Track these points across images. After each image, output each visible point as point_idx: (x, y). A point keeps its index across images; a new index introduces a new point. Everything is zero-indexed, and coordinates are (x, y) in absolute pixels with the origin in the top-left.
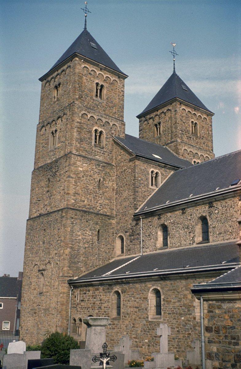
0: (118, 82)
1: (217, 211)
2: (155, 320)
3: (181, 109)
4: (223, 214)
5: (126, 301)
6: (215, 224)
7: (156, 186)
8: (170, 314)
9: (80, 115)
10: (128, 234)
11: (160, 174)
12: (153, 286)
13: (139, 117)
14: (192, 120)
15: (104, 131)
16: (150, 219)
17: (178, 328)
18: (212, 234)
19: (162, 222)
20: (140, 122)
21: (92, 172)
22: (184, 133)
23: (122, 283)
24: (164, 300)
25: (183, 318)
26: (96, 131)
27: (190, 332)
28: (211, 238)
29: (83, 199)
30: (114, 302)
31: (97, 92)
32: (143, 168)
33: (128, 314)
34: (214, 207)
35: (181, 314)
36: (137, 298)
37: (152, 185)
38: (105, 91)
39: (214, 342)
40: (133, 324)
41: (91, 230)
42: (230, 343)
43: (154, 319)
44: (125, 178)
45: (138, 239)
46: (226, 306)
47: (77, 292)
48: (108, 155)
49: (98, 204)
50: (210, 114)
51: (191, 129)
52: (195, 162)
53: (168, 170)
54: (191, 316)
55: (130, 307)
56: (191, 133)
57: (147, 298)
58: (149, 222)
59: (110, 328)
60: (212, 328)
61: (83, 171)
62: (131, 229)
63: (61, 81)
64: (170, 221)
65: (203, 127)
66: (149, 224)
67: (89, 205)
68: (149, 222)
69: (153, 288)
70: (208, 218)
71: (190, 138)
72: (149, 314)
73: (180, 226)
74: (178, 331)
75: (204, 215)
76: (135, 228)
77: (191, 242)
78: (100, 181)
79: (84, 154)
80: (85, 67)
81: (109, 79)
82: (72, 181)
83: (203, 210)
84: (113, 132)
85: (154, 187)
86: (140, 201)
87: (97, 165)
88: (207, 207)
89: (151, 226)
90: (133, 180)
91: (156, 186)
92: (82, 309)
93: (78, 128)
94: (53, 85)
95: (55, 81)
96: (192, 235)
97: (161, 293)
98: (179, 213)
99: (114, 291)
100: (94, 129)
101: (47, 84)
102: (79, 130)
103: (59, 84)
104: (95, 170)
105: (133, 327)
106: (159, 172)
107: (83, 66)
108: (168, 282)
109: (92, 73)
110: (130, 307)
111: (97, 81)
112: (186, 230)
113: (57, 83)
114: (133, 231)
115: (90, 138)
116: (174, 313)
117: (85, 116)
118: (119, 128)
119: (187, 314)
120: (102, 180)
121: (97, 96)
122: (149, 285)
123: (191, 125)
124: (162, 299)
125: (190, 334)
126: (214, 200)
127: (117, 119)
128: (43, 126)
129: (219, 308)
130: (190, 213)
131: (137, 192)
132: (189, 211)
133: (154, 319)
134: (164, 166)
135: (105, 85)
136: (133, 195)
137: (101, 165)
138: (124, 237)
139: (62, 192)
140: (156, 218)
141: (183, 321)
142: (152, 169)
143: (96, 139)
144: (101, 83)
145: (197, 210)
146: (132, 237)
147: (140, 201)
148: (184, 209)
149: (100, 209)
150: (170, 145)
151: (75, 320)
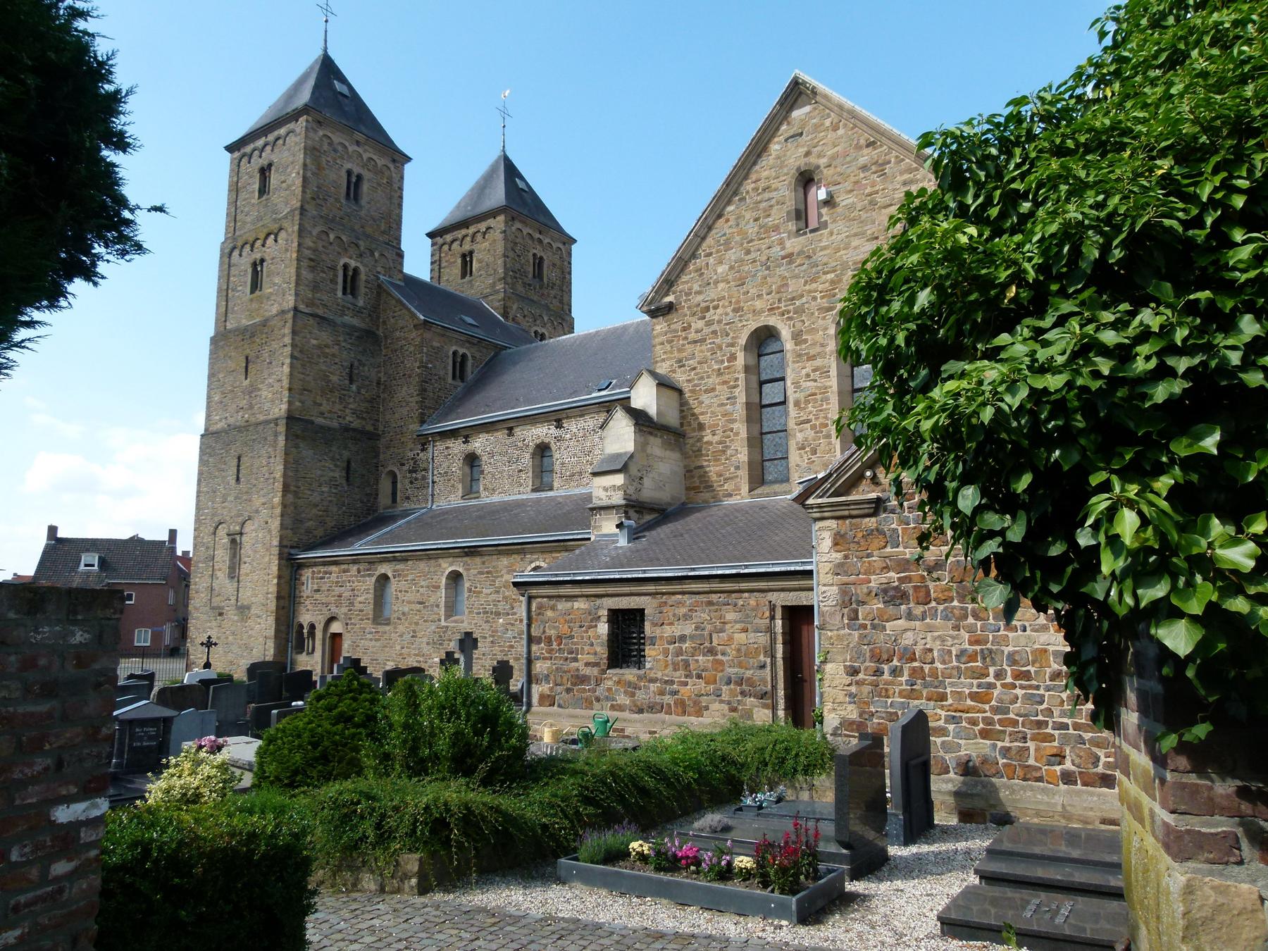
0: (392, 169)
3: (514, 228)
5: (400, 591)
7: (462, 379)
8: (479, 613)
9: (315, 233)
10: (406, 468)
11: (470, 358)
12: (451, 565)
13: (430, 235)
14: (535, 251)
15: (362, 268)
17: (493, 636)
20: (433, 245)
21: (336, 347)
22: (518, 276)
25: (501, 620)
26: (346, 267)
31: (348, 188)
32: (438, 345)
35: (498, 614)
36: (422, 587)
37: (454, 377)
38: (365, 187)
40: (414, 631)
44: (402, 362)
45: (424, 478)
46: (562, 606)
48: (370, 315)
49: (347, 411)
51: (531, 269)
52: (536, 332)
53: (485, 350)
55: (409, 602)
56: (531, 276)
59: (371, 640)
60: (541, 638)
61: (319, 347)
62: (412, 459)
63: (275, 158)
65: (554, 265)
67: (330, 412)
71: (530, 285)
74: (492, 642)
75: (546, 440)
78: (352, 365)
79: (320, 312)
80: (325, 135)
81: (373, 163)
83: (543, 432)
84: (379, 269)
85: (459, 383)
86: (430, 408)
87: (349, 334)
91: (462, 379)
93: (311, 260)
94: (257, 162)
95: (260, 157)
99: (378, 573)
100: (342, 263)
101: (245, 160)
102: (312, 264)
103: (270, 165)
104: (343, 344)
105: (413, 637)
106: (469, 355)
107: (321, 133)
108: (478, 560)
109: (340, 148)
110: (409, 602)
111: (348, 166)
113: (266, 163)
115: (334, 281)
116: (487, 613)
117: (324, 237)
118: (391, 262)
119: (508, 614)
120: (356, 364)
121: (348, 194)
123: (531, 261)
125: (512, 647)
126: (564, 416)
127: (388, 244)
128: (234, 248)
129: (553, 608)
135: (367, 175)
137: (356, 334)
138: (398, 473)
140: (460, 440)
141: (503, 625)
142: (454, 348)
143: (345, 281)
144: (356, 170)
146: (414, 475)
147: (430, 408)
149: (351, 420)
150: (491, 298)
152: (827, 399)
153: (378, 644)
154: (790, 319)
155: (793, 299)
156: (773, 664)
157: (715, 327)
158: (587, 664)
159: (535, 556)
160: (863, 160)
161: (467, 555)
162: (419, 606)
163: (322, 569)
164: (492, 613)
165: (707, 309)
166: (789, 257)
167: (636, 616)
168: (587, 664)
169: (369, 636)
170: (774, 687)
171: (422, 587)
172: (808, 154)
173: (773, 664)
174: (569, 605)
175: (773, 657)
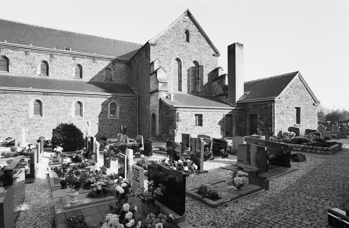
1: (56, 61)
2: (35, 118)
6: (54, 67)
18: (51, 72)
24: (45, 106)
33: (4, 114)
36: (17, 104)
54: (68, 116)
55: (8, 109)
64: (11, 56)
72: (29, 114)
75: (46, 60)
77: (33, 74)
96: (34, 70)
108: (49, 97)
122: (29, 96)
132: (32, 54)
148: (28, 52)
154: (182, 58)
156: (224, 124)
157: (166, 54)
160: (197, 34)
161: (44, 94)
162: (14, 111)
165: (165, 49)
166: (183, 46)
167: (201, 115)
170: (224, 128)
171: (17, 104)
172: (187, 27)
173: (224, 124)
175: (224, 123)
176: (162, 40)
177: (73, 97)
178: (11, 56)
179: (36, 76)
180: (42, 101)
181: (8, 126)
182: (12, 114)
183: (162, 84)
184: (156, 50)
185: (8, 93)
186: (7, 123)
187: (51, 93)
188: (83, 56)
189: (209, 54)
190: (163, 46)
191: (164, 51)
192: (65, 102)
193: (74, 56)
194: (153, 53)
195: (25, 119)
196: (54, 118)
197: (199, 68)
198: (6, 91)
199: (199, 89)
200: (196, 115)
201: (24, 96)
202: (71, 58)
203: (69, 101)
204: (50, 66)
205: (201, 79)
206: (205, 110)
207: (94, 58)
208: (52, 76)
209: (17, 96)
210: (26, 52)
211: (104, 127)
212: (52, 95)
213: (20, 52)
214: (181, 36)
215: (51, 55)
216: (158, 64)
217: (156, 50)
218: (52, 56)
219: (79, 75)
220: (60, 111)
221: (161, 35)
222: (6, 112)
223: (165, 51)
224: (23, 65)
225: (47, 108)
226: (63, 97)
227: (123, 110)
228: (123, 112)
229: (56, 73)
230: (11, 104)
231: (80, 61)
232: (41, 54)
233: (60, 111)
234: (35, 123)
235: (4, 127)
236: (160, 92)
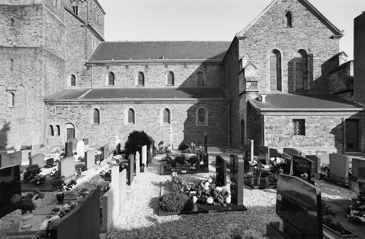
1: (150, 71)
4: (154, 73)
6: (149, 77)
10: (80, 74)
16: (100, 67)
19: (110, 71)
23: (102, 103)
24: (137, 115)
27: (156, 131)
28: (145, 84)
29: (50, 44)
30: (92, 115)
33: (106, 122)
34: (149, 68)
36: (115, 113)
39: (270, 133)
40: (111, 128)
41: (55, 67)
42: (278, 133)
43: (129, 125)
47: (52, 108)
50: (104, 13)
54: (156, 123)
55: (109, 118)
57: (123, 113)
58: (99, 69)
59: (89, 131)
64: (116, 71)
66: (98, 70)
68: (99, 69)
69: (128, 108)
70: (144, 73)
72: (124, 122)
73: (124, 75)
75: (142, 71)
76: (86, 71)
77: (132, 85)
82: (44, 28)
88: (144, 68)
89: (100, 71)
90: (85, 40)
92: (60, 119)
96: (133, 81)
97: (135, 111)
98: (123, 67)
108: (140, 105)
112: (128, 78)
114: (84, 73)
122: (124, 105)
124: (135, 114)
125: (155, 132)
130: (132, 69)
131: (87, 49)
132: (131, 67)
133: (129, 125)
134: (98, 37)
136: (84, 50)
139: (33, 34)
145: (137, 68)
151: (51, 127)
152: (292, 71)
153: (93, 132)
154: (282, 49)
155: (283, 44)
156: (343, 133)
157: (260, 47)
158: (285, 134)
159: (164, 105)
160: (304, 13)
161: (136, 103)
162: (113, 120)
163: (62, 106)
164: (146, 122)
165: (257, 41)
166: (282, 33)
168: (285, 134)
169: (88, 129)
170: (343, 138)
172: (289, 7)
173: (343, 133)
174: (279, 118)
175: (343, 131)
176: (254, 31)
177: (162, 105)
178: (116, 71)
179: (134, 87)
180: (135, 110)
181: (109, 133)
182: (112, 122)
183: (251, 83)
184: (246, 44)
185: (109, 104)
186: (108, 130)
187: (141, 102)
188: (174, 63)
189: (324, 37)
190: (255, 38)
191: (256, 43)
192: (154, 110)
193: (166, 64)
194: (242, 48)
195: (121, 127)
196: (145, 126)
197: (307, 58)
198: (107, 102)
199: (307, 87)
200: (295, 120)
201: (120, 105)
202: (164, 66)
203: (158, 108)
204: (145, 76)
205: (310, 73)
206: (309, 113)
207: (185, 64)
208: (147, 85)
209: (115, 106)
210: (126, 66)
211: (191, 135)
212: (142, 103)
213: (122, 67)
214: (279, 21)
215: (146, 66)
216: (248, 60)
217: (246, 44)
218: (147, 67)
219: (171, 81)
220: (149, 118)
221: (252, 25)
222: (107, 121)
223: (258, 43)
224: (124, 78)
225: (138, 116)
226: (152, 105)
227: (212, 117)
228: (211, 119)
229: (150, 82)
230: (111, 113)
231: (172, 68)
232: (138, 66)
233: (149, 118)
234: (128, 130)
235: (106, 133)
236: (249, 93)
